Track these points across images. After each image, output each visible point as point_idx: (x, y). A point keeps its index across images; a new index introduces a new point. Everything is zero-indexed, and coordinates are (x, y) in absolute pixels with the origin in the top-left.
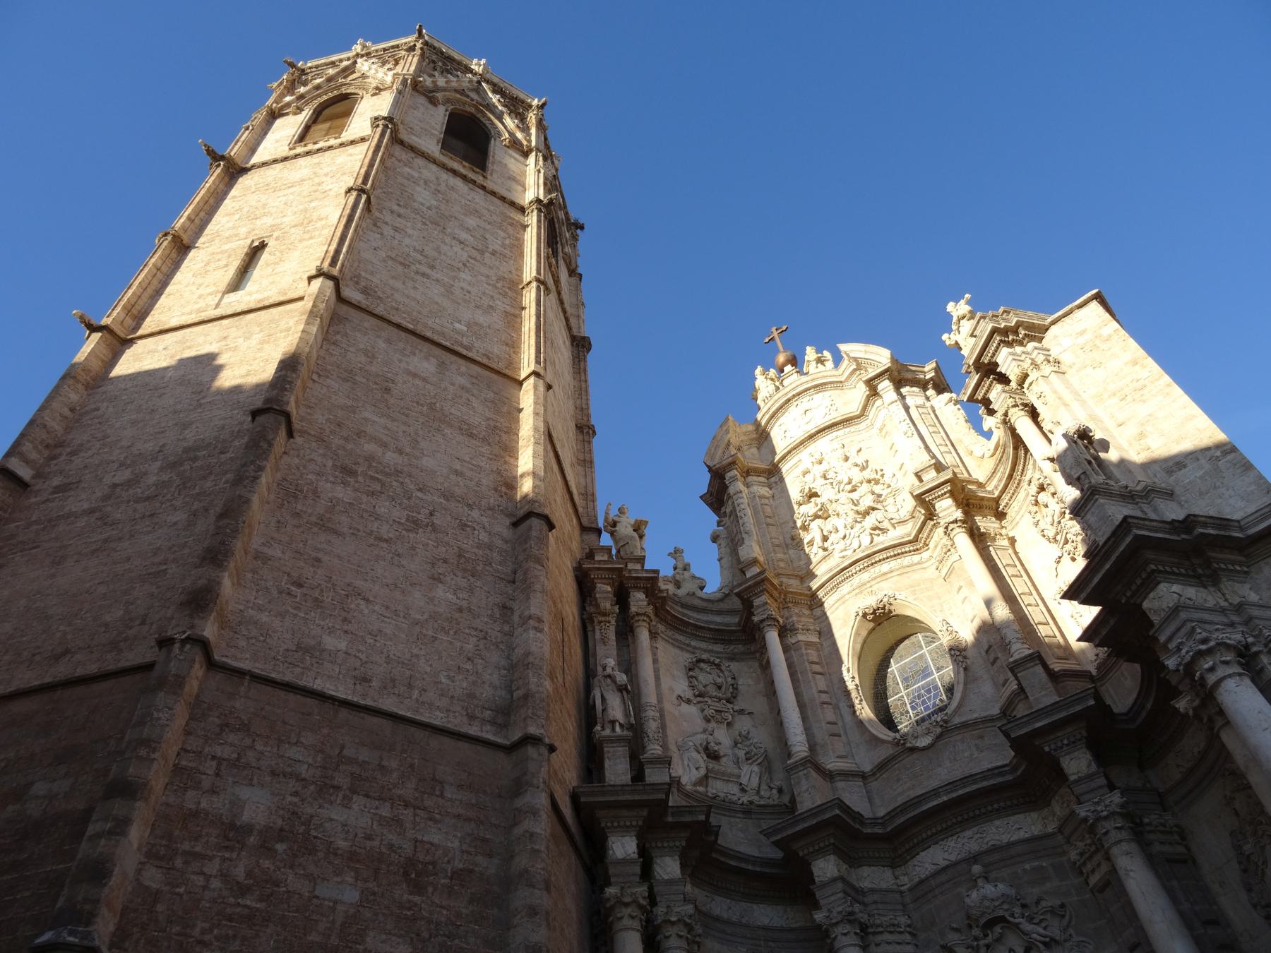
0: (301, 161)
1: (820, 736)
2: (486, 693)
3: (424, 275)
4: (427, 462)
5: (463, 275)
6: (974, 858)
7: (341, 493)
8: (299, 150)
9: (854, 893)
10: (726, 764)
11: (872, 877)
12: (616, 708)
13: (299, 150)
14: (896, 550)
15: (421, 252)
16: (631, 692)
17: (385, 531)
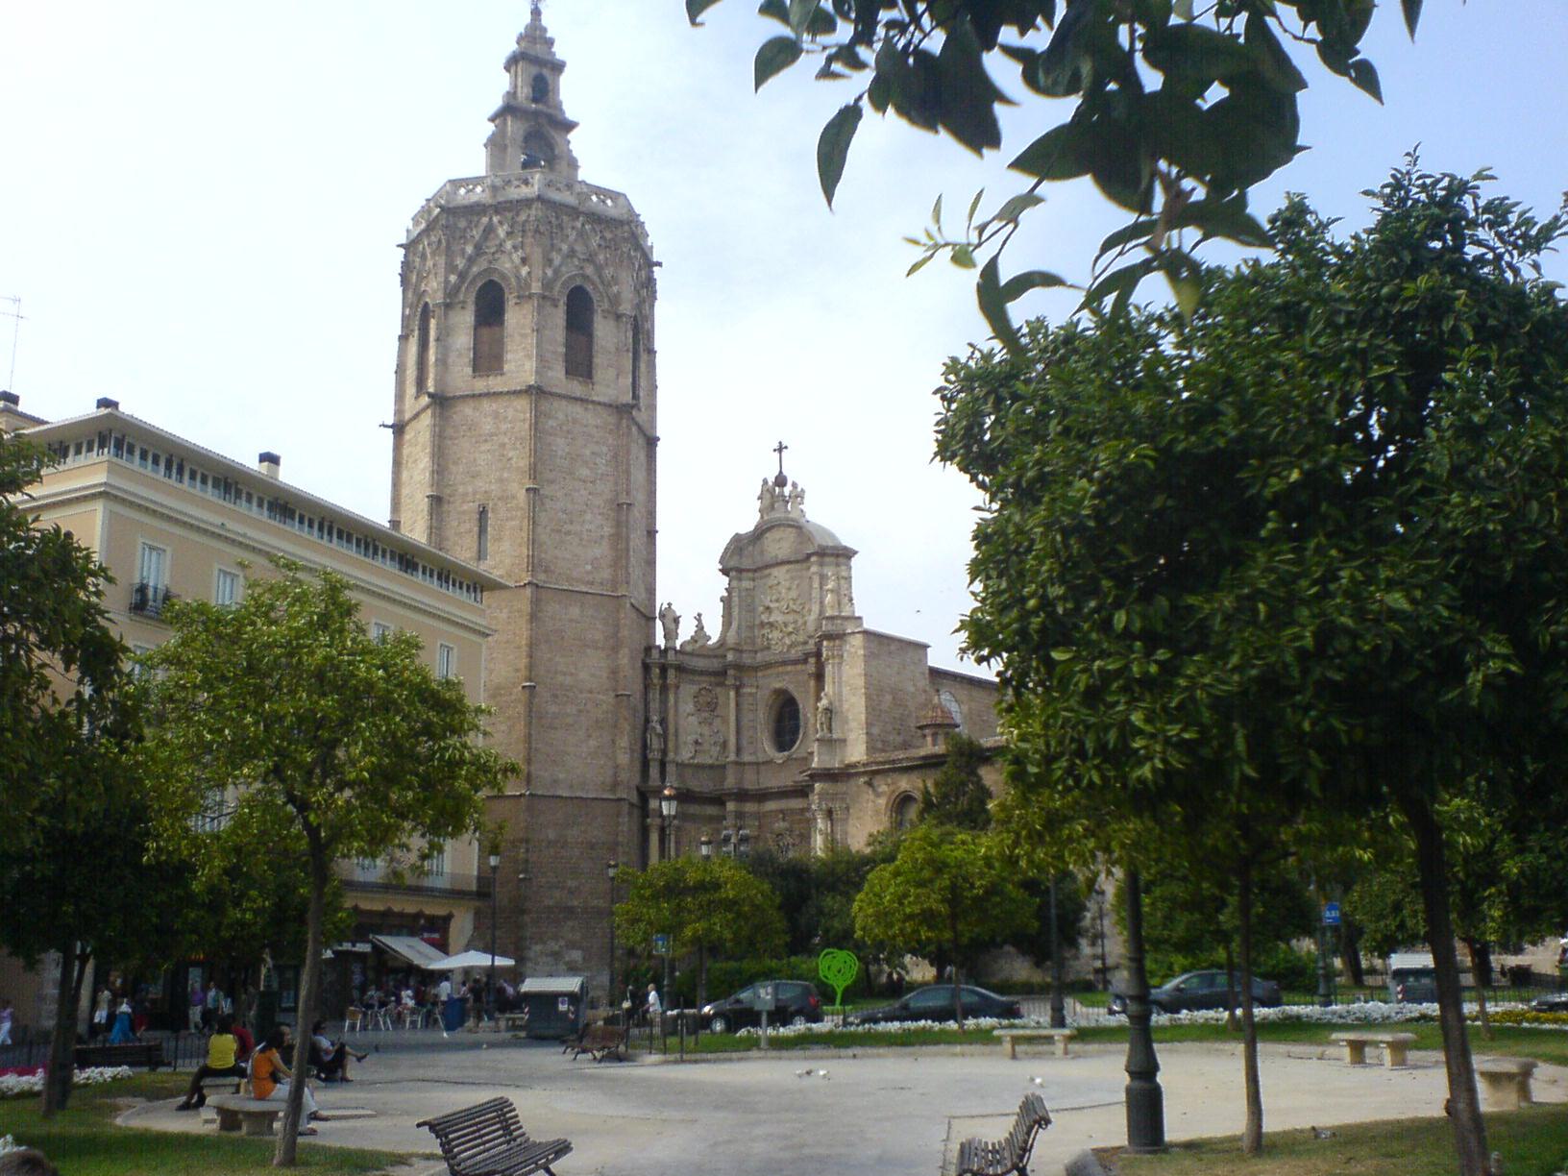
0: (487, 405)
1: (744, 742)
2: (609, 780)
3: (568, 533)
4: (583, 675)
5: (588, 517)
6: (782, 811)
7: (553, 709)
8: (480, 385)
9: (740, 815)
10: (706, 747)
11: (750, 807)
12: (655, 744)
13: (480, 385)
14: (795, 662)
15: (564, 511)
16: (665, 736)
17: (570, 720)
